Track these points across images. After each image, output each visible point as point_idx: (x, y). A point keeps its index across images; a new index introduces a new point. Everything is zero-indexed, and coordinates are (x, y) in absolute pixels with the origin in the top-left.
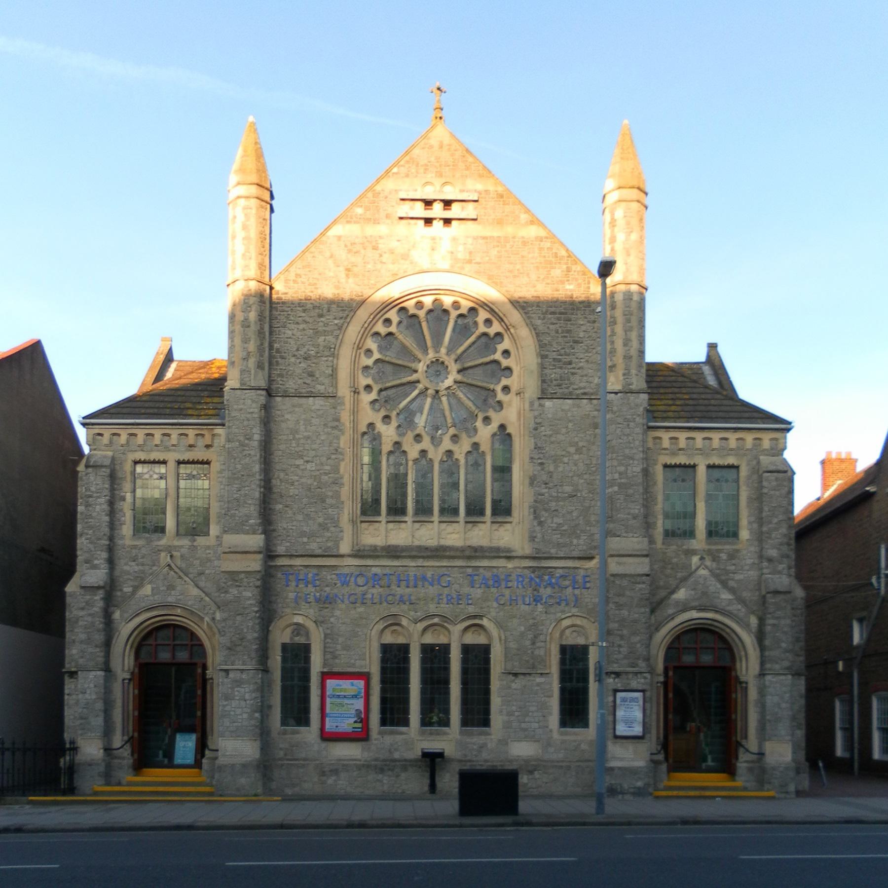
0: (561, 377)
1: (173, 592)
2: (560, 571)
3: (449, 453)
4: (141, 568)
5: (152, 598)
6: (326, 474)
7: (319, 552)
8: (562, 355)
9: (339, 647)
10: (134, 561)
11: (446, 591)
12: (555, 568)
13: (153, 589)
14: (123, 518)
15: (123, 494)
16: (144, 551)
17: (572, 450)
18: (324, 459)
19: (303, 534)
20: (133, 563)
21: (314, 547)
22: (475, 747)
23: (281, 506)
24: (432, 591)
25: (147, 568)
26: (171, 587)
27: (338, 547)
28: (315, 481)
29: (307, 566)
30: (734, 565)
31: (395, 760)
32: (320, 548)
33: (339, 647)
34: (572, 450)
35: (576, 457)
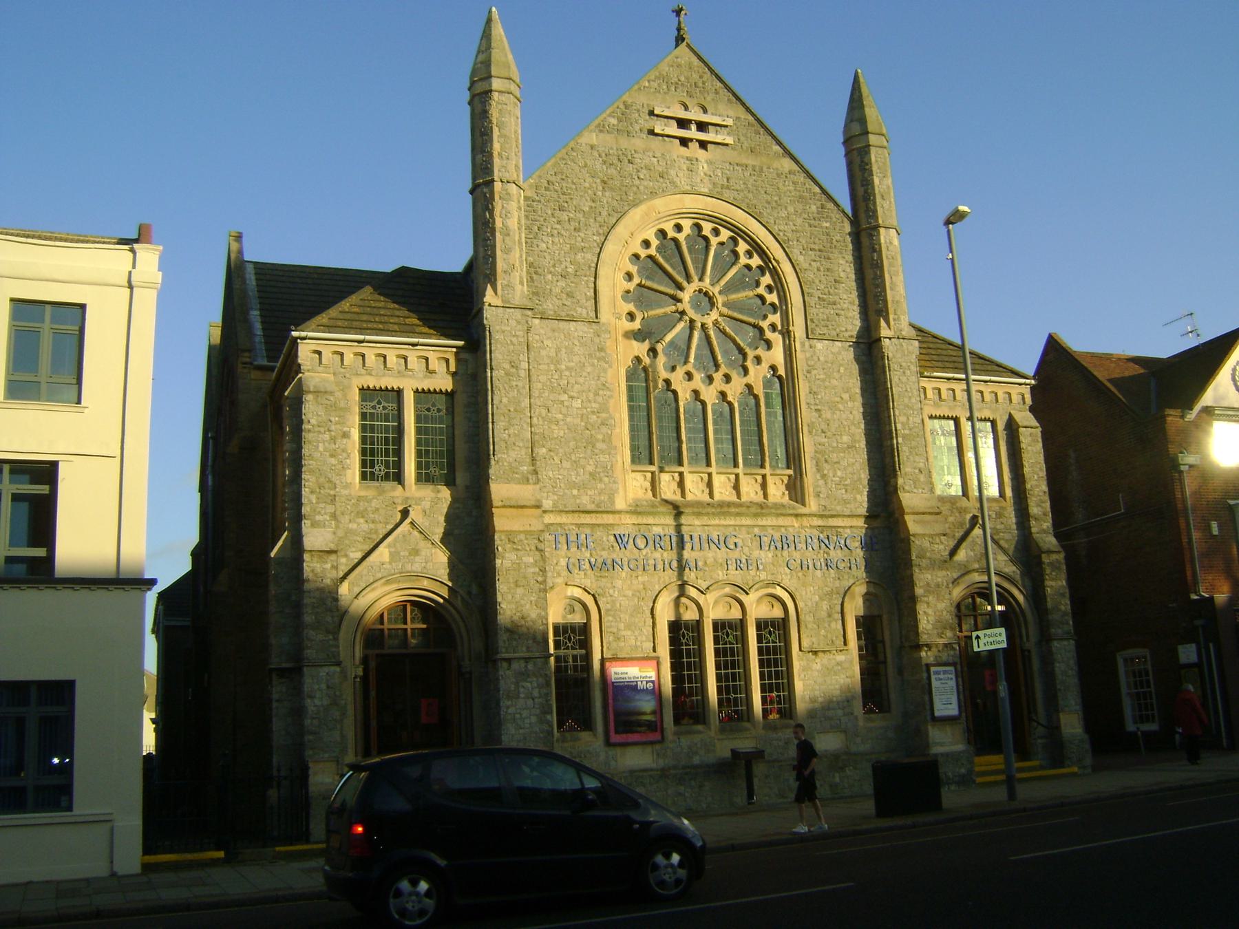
0: (828, 318)
1: (417, 559)
2: (848, 531)
3: (723, 395)
4: (372, 526)
5: (387, 566)
6: (593, 412)
7: (591, 507)
8: (825, 294)
9: (622, 626)
10: (363, 517)
11: (735, 554)
12: (843, 527)
13: (391, 553)
14: (348, 461)
15: (345, 429)
16: (374, 504)
17: (846, 396)
18: (591, 395)
19: (573, 485)
20: (362, 520)
21: (586, 501)
22: (780, 743)
23: (544, 450)
24: (722, 554)
25: (380, 526)
26: (416, 552)
27: (613, 503)
28: (582, 420)
29: (579, 526)
30: (1002, 523)
31: (696, 767)
32: (593, 502)
33: (622, 626)
34: (846, 396)
35: (850, 404)
